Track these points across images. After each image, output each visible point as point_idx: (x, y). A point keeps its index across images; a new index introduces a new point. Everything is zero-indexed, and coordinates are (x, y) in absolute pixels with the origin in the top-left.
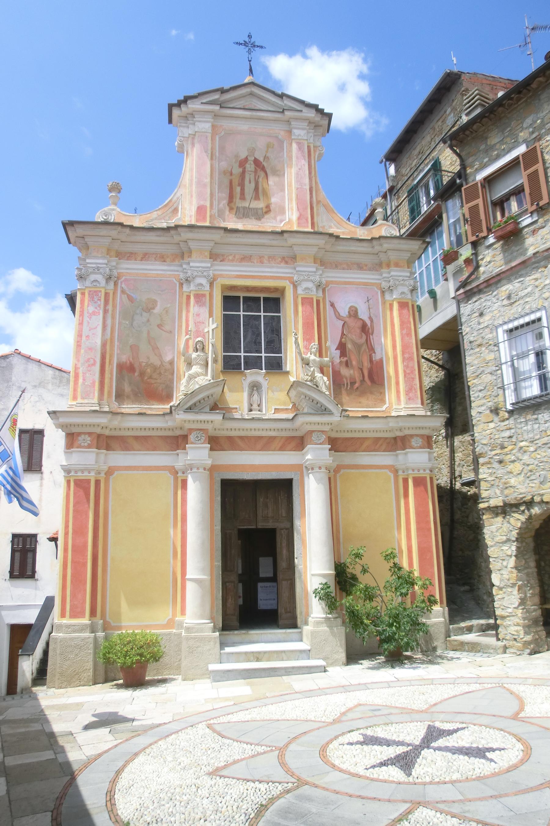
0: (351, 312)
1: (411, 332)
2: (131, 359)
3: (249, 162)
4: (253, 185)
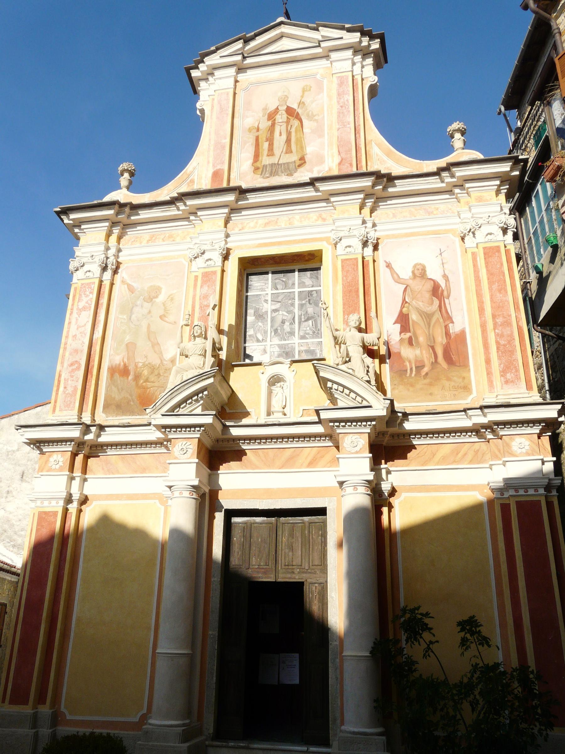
0: (416, 272)
1: (506, 286)
2: (126, 360)
3: (280, 113)
4: (284, 137)
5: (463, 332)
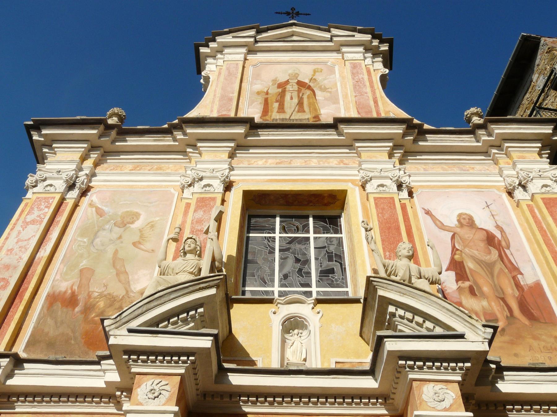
0: (462, 221)
2: (75, 288)
4: (296, 100)
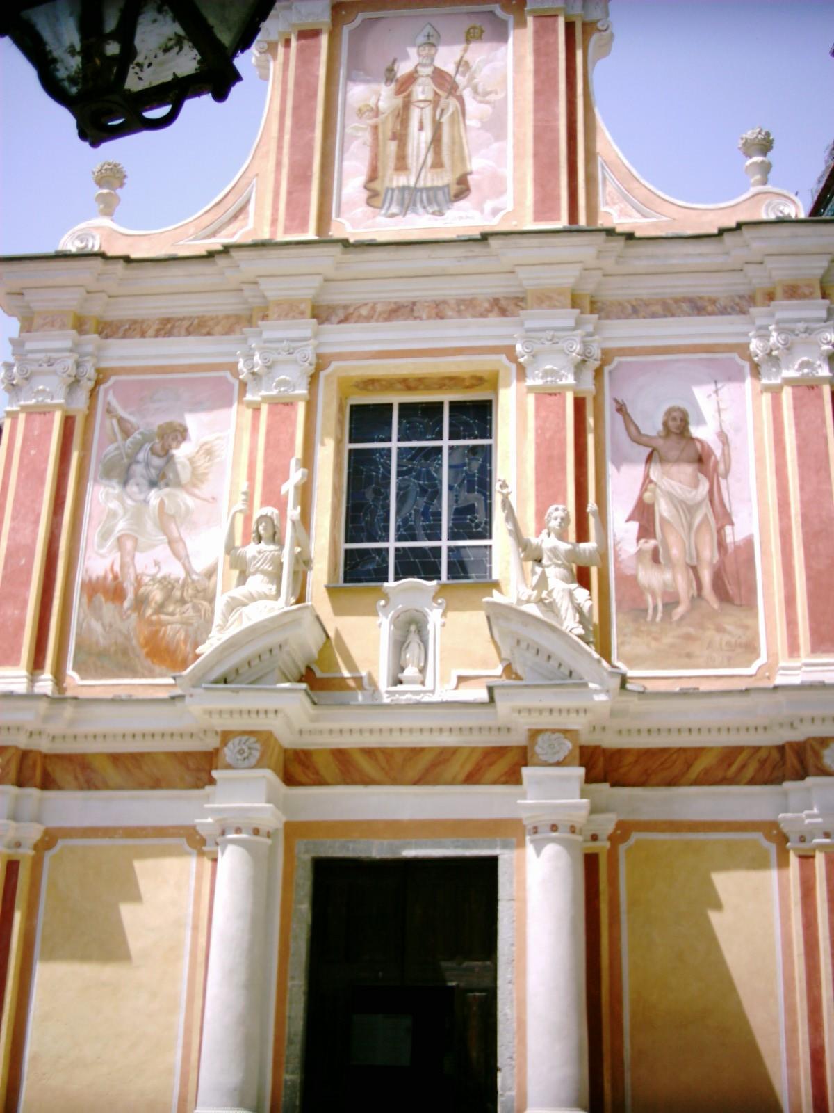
0: (671, 424)
2: (117, 568)
3: (420, 80)
4: (427, 135)
5: (749, 542)
